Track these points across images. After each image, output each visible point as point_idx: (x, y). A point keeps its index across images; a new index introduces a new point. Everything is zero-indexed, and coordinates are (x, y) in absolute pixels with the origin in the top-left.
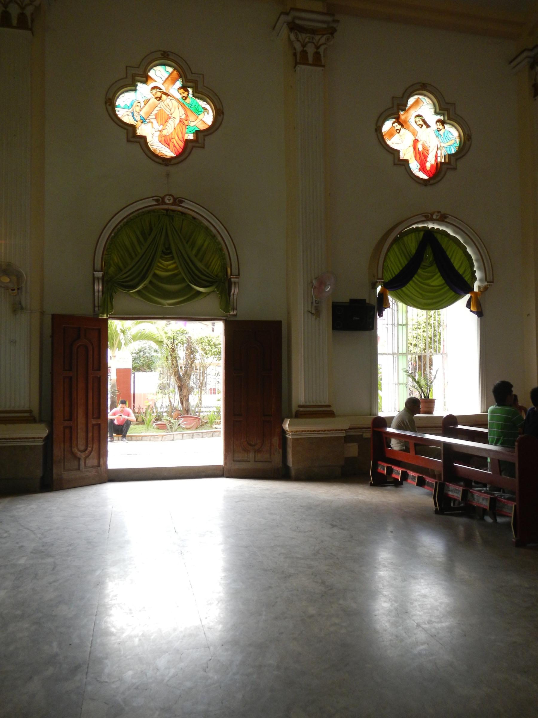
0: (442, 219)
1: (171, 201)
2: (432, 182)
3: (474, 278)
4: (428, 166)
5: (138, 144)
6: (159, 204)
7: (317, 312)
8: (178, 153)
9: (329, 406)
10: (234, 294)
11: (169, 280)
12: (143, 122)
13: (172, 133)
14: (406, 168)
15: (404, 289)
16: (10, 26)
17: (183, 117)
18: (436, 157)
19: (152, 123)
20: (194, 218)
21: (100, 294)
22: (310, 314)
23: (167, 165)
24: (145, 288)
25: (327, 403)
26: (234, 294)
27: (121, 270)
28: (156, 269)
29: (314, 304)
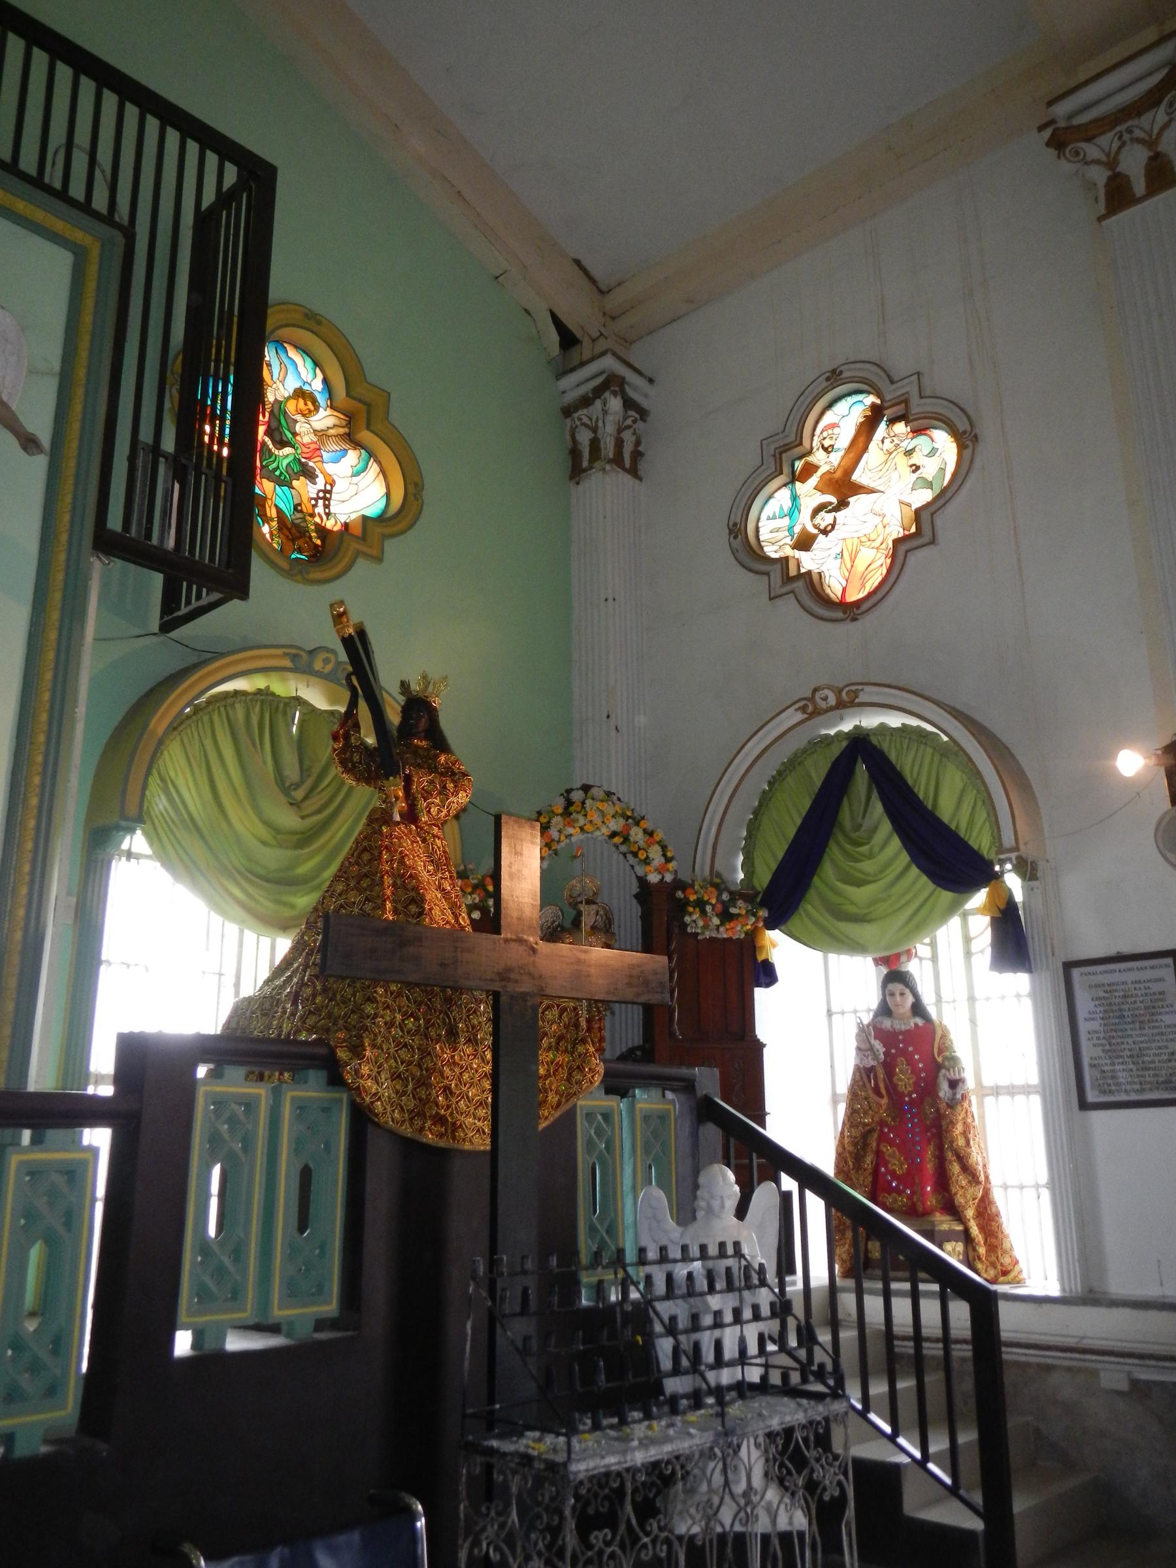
16: (1133, 201)
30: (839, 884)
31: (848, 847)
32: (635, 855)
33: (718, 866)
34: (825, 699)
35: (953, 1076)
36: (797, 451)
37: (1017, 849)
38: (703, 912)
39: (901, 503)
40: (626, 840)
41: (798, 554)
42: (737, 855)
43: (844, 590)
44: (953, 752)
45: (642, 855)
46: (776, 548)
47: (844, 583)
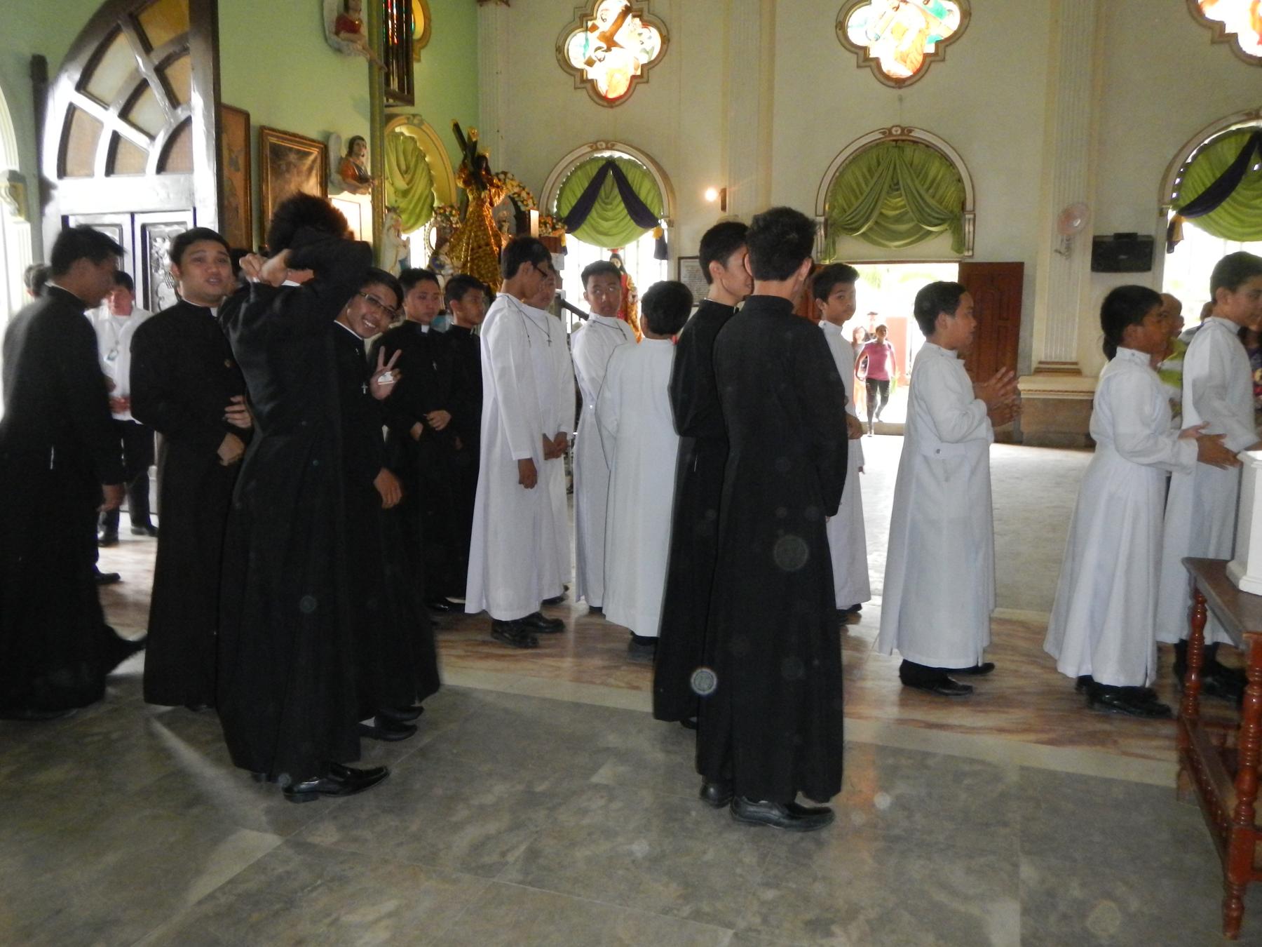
1: (899, 132)
6: (886, 137)
7: (1066, 250)
9: (1076, 363)
10: (969, 232)
11: (898, 219)
12: (877, 40)
17: (923, 26)
20: (927, 146)
21: (823, 239)
24: (870, 229)
25: (1074, 360)
26: (969, 232)
28: (883, 208)
30: (600, 220)
31: (603, 205)
32: (522, 202)
33: (549, 206)
34: (601, 145)
35: (634, 294)
36: (589, 18)
37: (669, 217)
38: (546, 227)
40: (519, 195)
42: (553, 201)
44: (647, 174)
45: (525, 203)
47: (607, 88)
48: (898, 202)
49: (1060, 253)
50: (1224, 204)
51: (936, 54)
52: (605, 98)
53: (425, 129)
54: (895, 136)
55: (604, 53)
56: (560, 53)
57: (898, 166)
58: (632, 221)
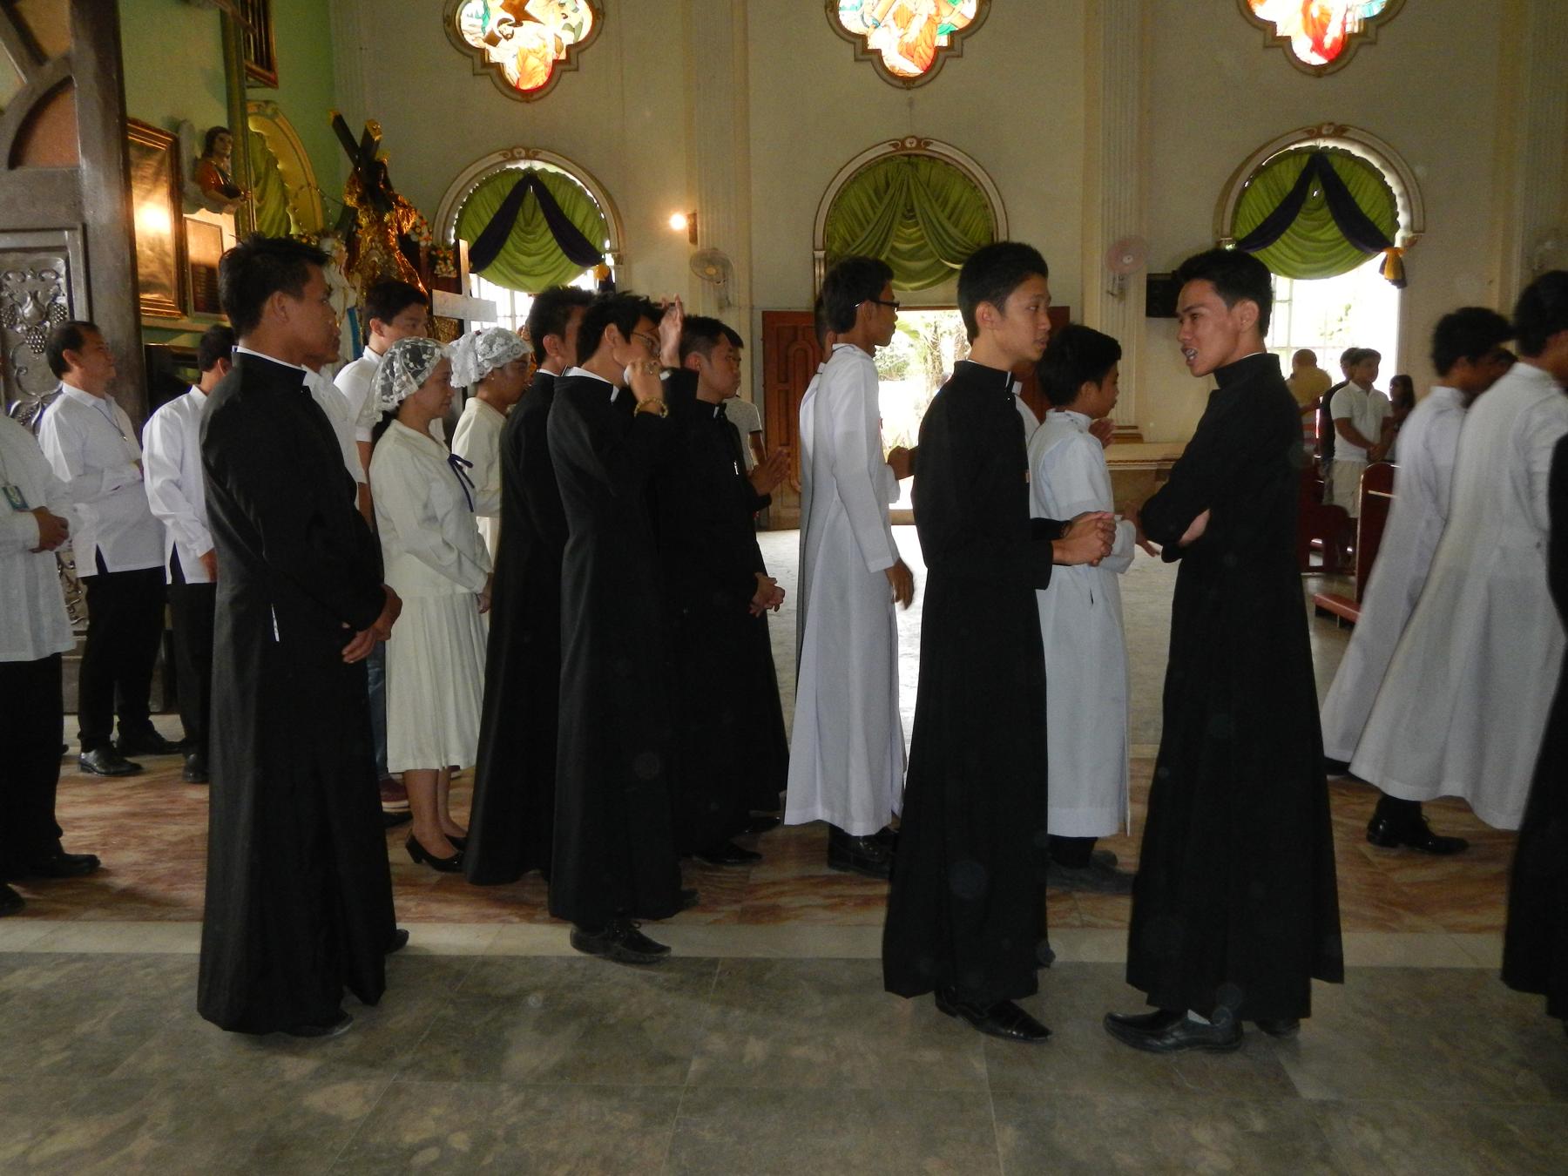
0: (1339, 132)
1: (914, 145)
2: (1330, 70)
3: (1396, 226)
4: (1328, 42)
5: (869, 64)
6: (898, 150)
7: (1120, 293)
8: (925, 67)
9: (1136, 427)
11: (912, 255)
12: (876, 28)
13: (917, 39)
14: (1285, 53)
15: (1271, 248)
17: (933, 12)
18: (1344, 24)
19: (889, 27)
20: (947, 164)
22: (1110, 296)
23: (909, 89)
25: (1133, 424)
27: (849, 245)
28: (895, 241)
29: (1117, 281)
30: (517, 254)
31: (522, 234)
34: (520, 153)
37: (619, 250)
38: (446, 264)
39: (556, 35)
41: (488, 47)
42: (451, 228)
43: (518, 79)
46: (473, 37)
47: (519, 75)
48: (911, 234)
49: (1112, 294)
50: (1284, 237)
51: (950, 47)
52: (516, 89)
53: (280, 123)
54: (910, 149)
55: (512, 28)
56: (449, 25)
57: (912, 188)
58: (565, 256)
